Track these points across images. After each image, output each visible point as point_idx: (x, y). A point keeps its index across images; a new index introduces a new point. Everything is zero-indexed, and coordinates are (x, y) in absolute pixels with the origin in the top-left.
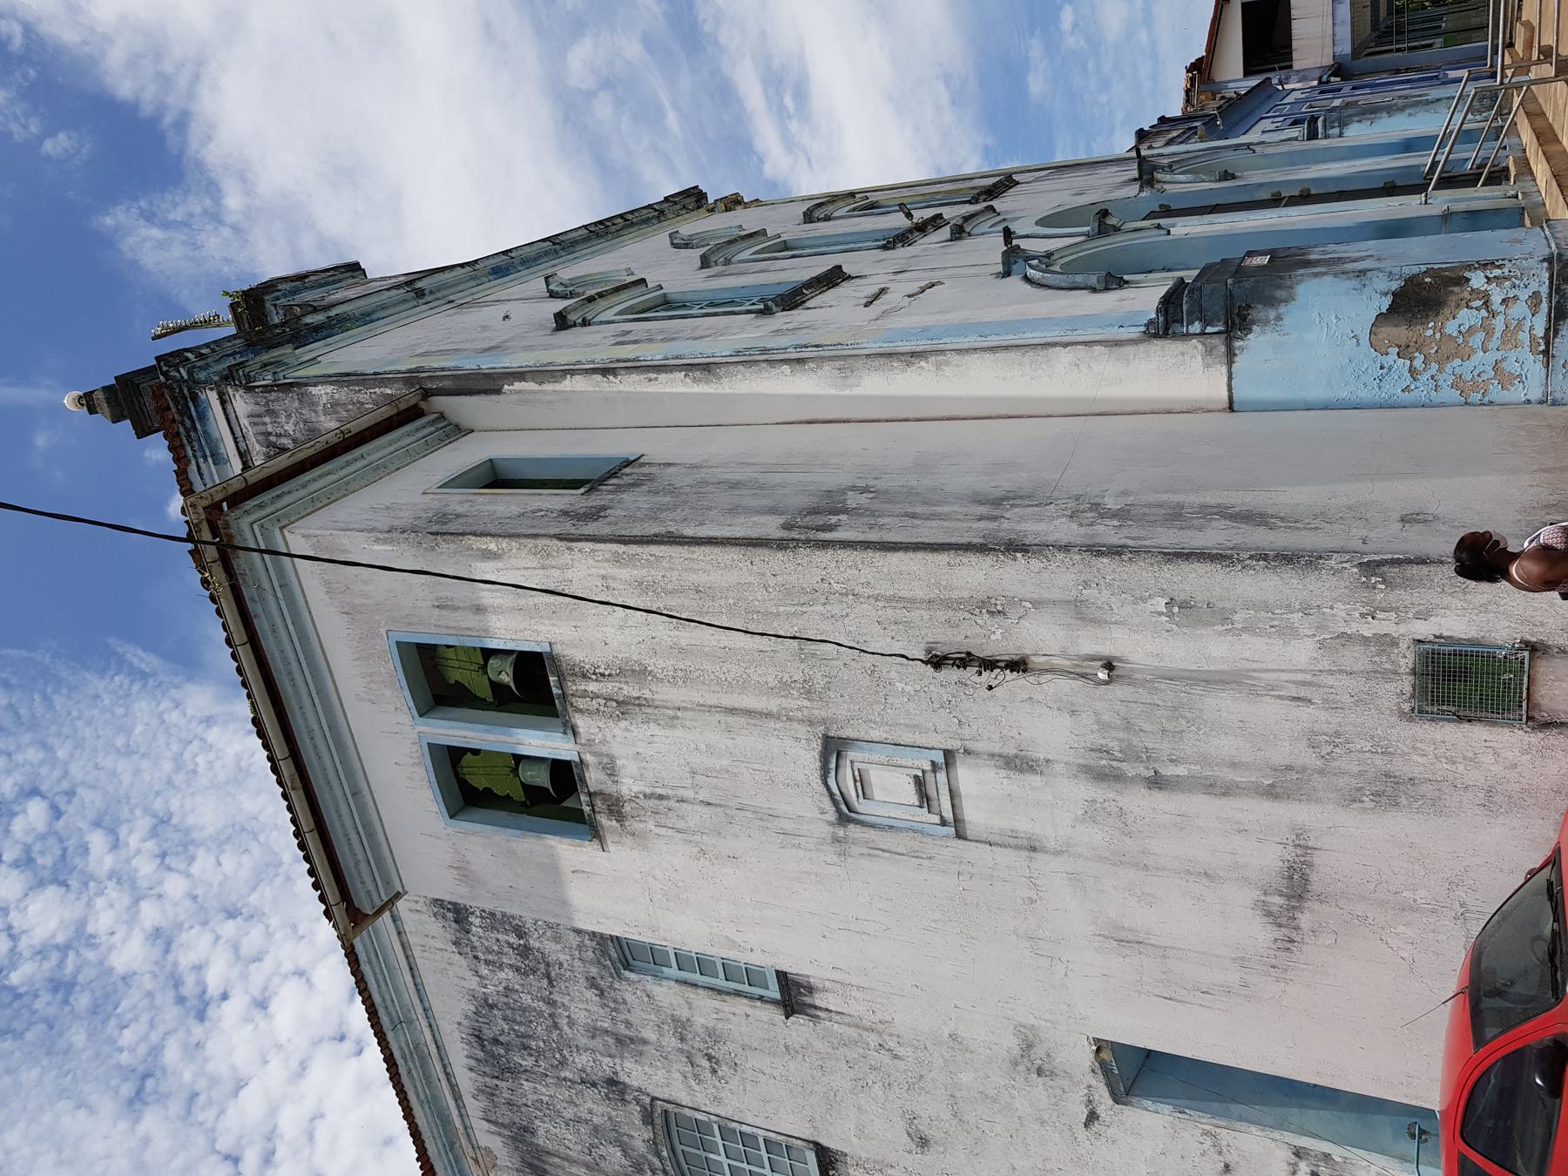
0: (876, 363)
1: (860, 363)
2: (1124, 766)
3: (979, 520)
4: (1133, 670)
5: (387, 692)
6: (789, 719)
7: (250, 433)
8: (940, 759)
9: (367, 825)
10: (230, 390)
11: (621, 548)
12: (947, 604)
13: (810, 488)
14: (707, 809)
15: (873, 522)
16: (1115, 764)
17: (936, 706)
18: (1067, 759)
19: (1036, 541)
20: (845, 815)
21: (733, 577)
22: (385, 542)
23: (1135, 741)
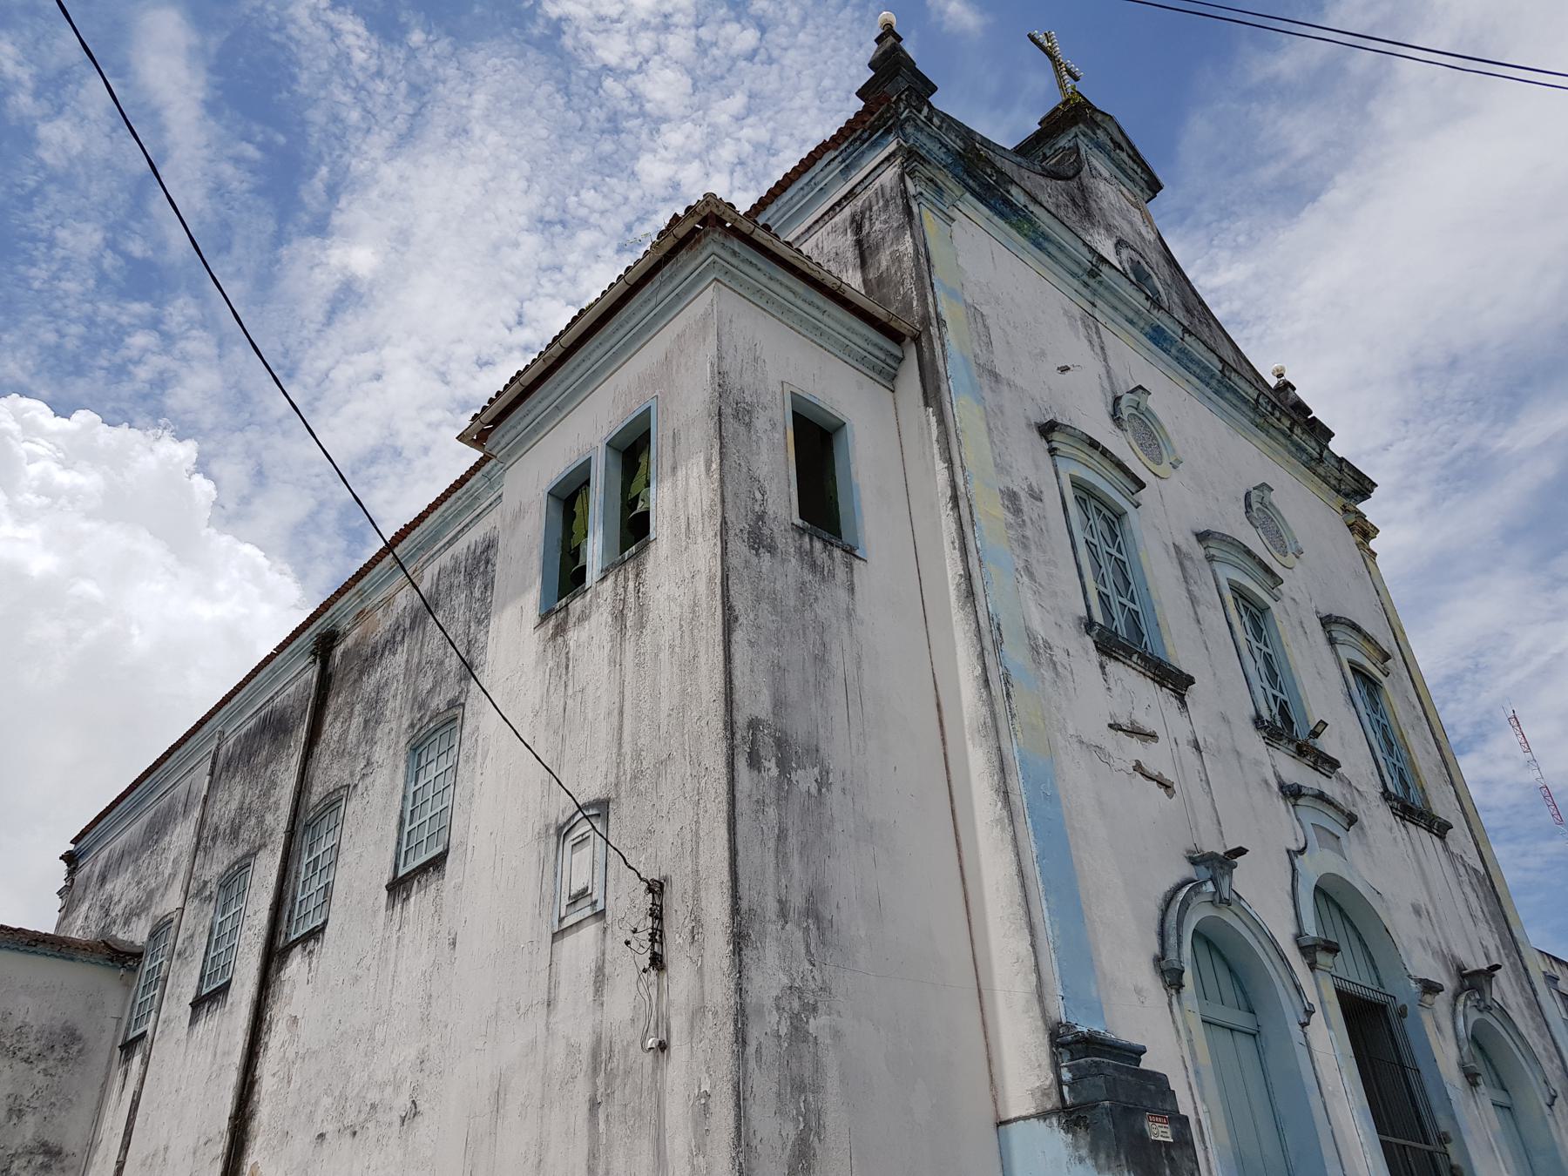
0: (995, 758)
1: (992, 742)
2: (603, 1074)
3: (780, 901)
4: (662, 1069)
5: (620, 411)
6: (618, 766)
7: (869, 192)
8: (599, 907)
9: (541, 425)
10: (899, 161)
11: (718, 581)
12: (696, 890)
13: (821, 731)
14: (562, 709)
15: (767, 801)
16: (603, 1065)
17: (632, 895)
18: (604, 1022)
19: (745, 959)
20: (563, 831)
21: (705, 688)
22: (712, 372)
23: (618, 1081)
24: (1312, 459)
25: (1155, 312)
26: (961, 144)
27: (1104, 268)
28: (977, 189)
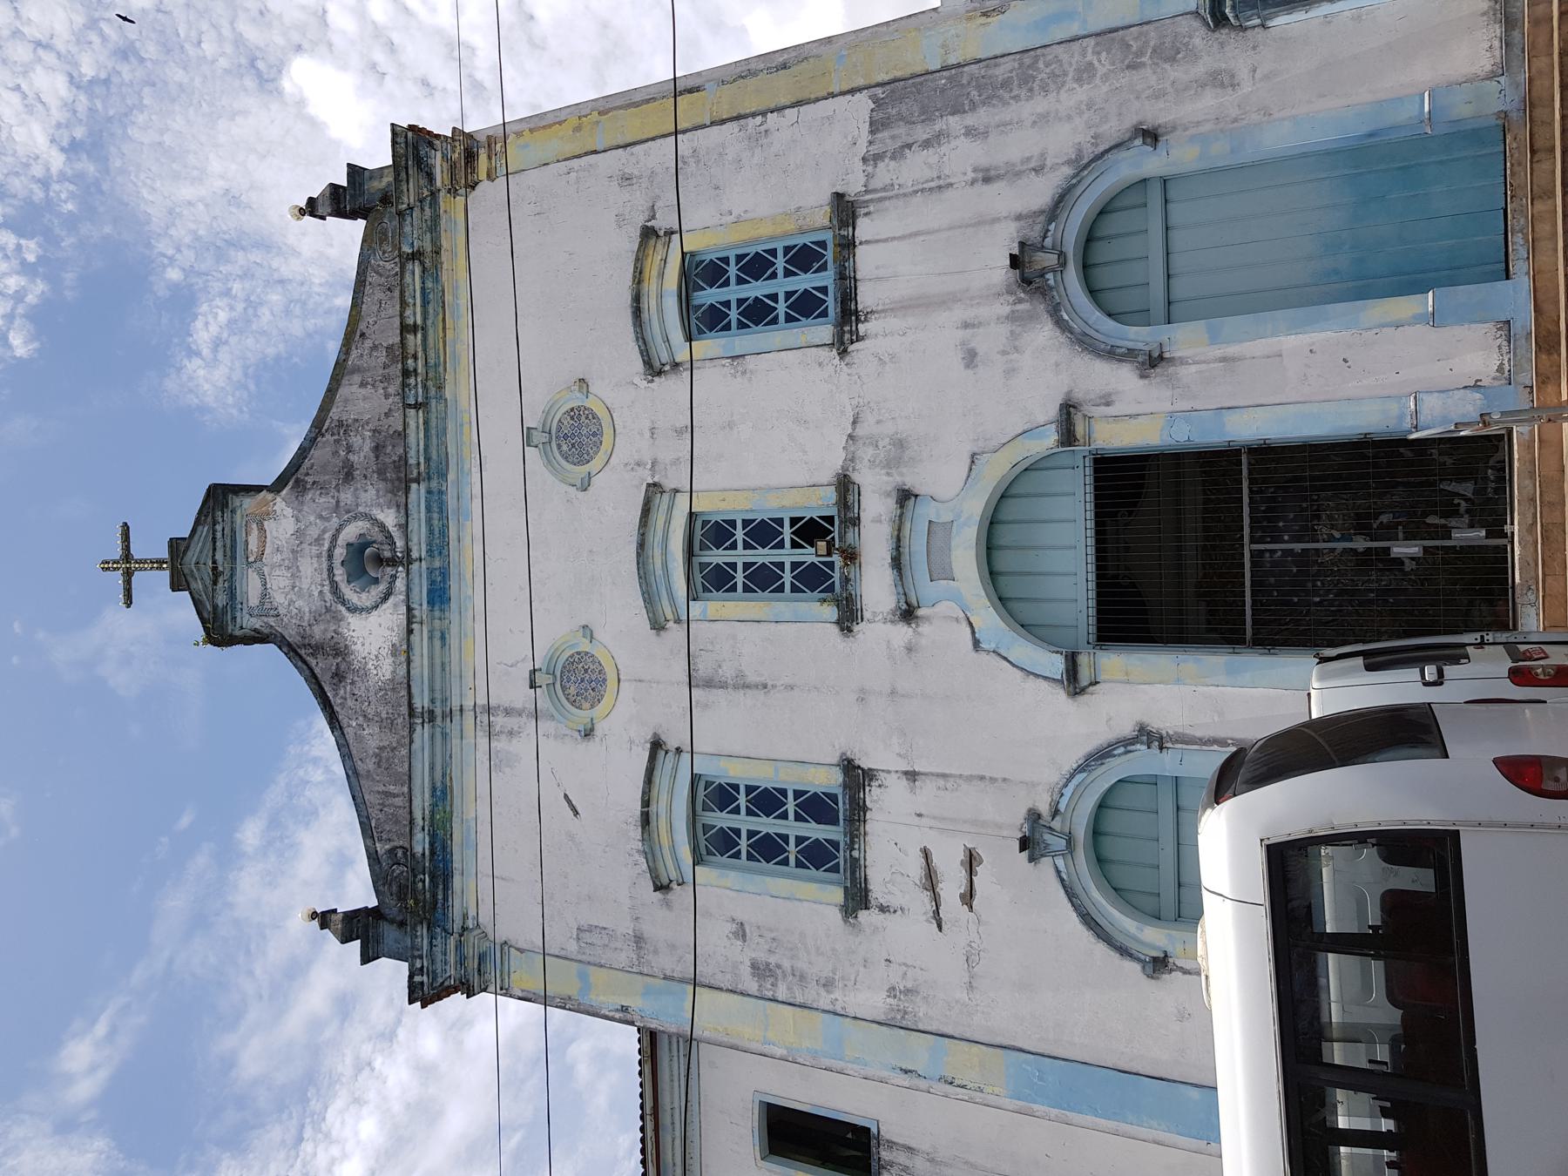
24: (424, 270)
25: (416, 613)
26: (419, 928)
27: (417, 703)
28: (441, 887)
